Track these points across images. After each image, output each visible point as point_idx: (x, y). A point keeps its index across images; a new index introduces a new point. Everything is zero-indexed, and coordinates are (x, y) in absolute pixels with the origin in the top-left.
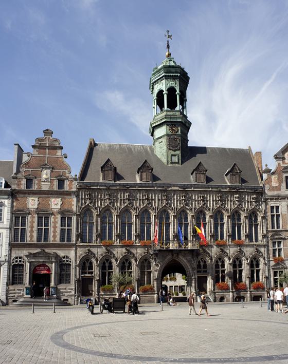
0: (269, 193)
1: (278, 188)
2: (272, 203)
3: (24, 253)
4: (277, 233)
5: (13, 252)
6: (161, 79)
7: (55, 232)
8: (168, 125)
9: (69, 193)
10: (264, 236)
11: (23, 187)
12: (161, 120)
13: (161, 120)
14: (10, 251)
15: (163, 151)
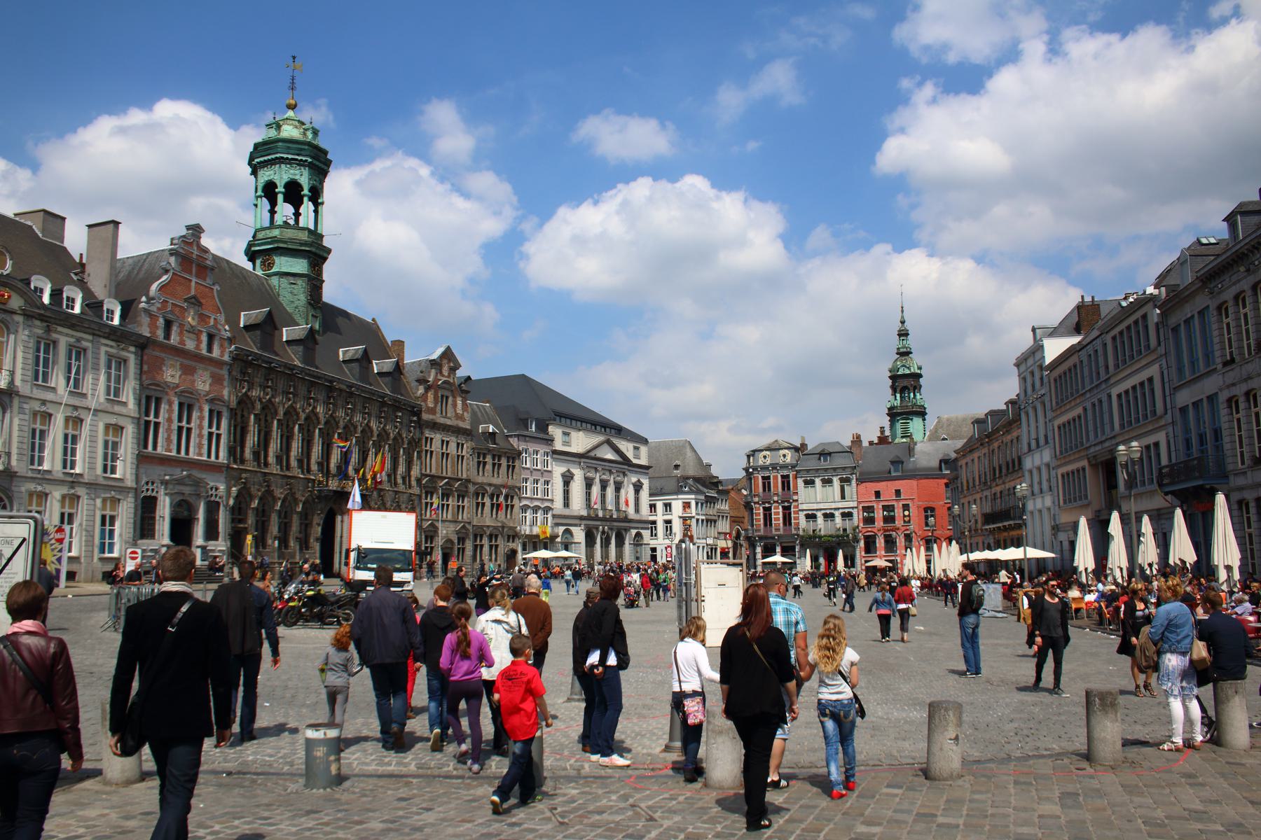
0: (425, 416)
1: (432, 411)
2: (428, 433)
3: (158, 472)
4: (433, 478)
5: (142, 471)
6: (301, 164)
7: (200, 436)
8: (309, 258)
9: (218, 363)
10: (419, 481)
11: (160, 334)
12: (302, 244)
13: (302, 244)
14: (138, 467)
15: (297, 303)
